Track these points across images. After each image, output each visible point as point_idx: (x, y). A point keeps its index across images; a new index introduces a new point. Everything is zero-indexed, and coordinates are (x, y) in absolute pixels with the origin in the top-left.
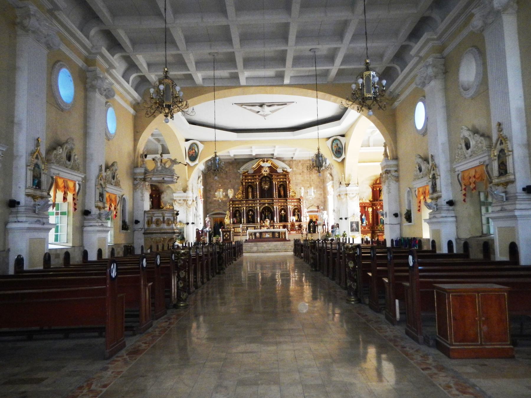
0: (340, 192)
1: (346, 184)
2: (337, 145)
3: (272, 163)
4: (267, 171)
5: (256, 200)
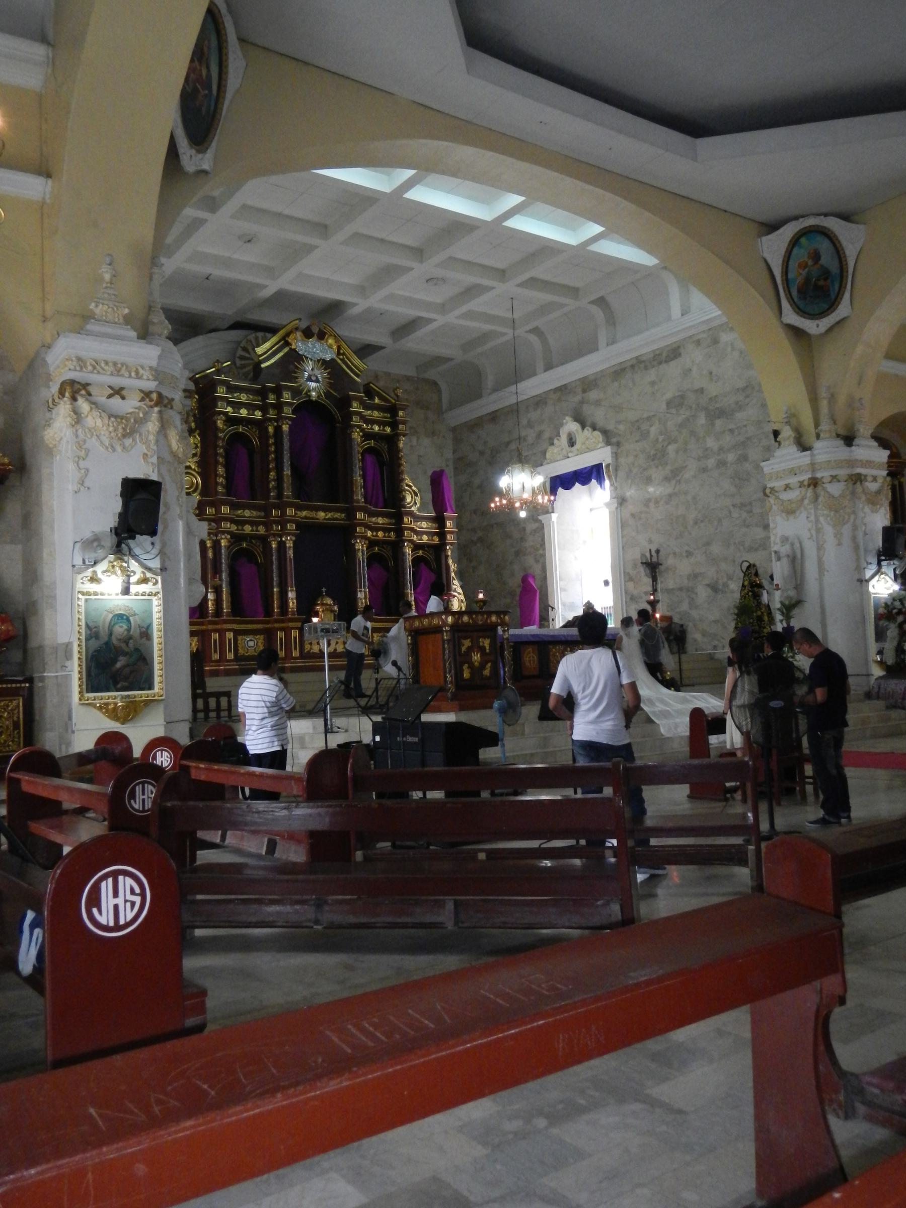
0: (814, 471)
1: (838, 436)
2: (816, 256)
3: (339, 348)
4: (317, 381)
5: (282, 507)
